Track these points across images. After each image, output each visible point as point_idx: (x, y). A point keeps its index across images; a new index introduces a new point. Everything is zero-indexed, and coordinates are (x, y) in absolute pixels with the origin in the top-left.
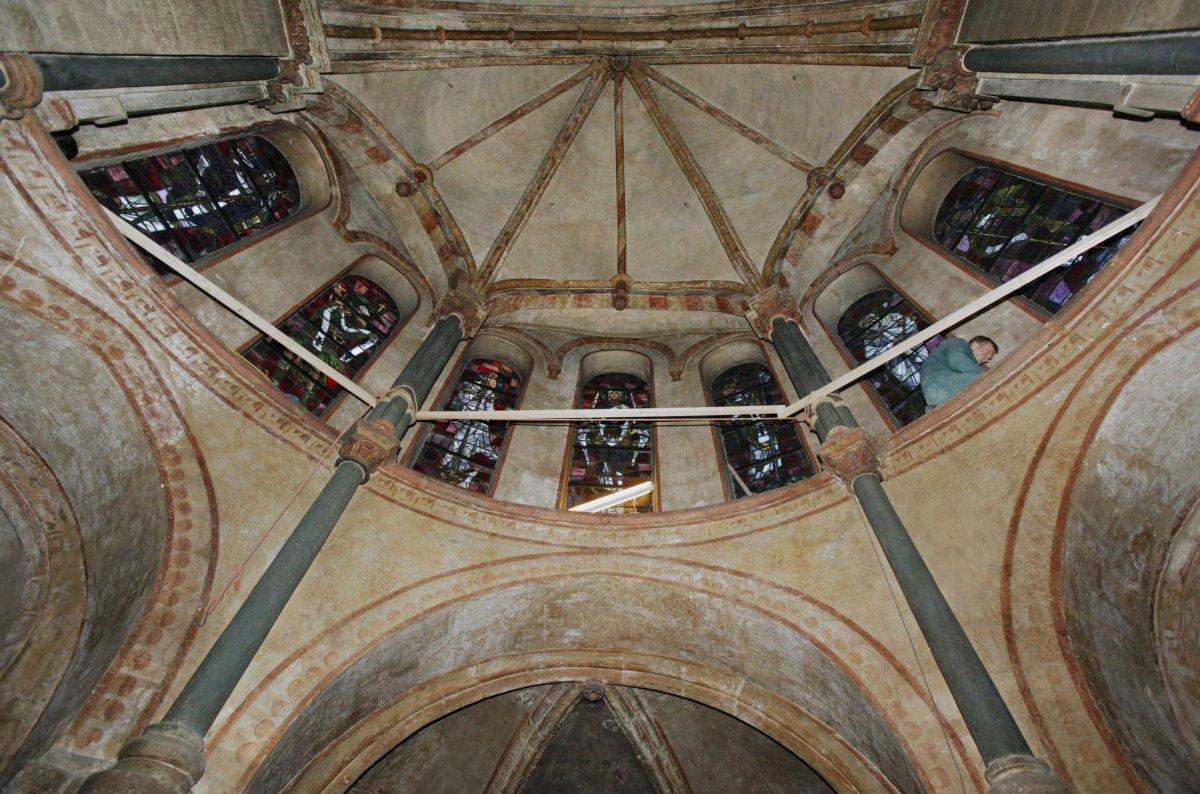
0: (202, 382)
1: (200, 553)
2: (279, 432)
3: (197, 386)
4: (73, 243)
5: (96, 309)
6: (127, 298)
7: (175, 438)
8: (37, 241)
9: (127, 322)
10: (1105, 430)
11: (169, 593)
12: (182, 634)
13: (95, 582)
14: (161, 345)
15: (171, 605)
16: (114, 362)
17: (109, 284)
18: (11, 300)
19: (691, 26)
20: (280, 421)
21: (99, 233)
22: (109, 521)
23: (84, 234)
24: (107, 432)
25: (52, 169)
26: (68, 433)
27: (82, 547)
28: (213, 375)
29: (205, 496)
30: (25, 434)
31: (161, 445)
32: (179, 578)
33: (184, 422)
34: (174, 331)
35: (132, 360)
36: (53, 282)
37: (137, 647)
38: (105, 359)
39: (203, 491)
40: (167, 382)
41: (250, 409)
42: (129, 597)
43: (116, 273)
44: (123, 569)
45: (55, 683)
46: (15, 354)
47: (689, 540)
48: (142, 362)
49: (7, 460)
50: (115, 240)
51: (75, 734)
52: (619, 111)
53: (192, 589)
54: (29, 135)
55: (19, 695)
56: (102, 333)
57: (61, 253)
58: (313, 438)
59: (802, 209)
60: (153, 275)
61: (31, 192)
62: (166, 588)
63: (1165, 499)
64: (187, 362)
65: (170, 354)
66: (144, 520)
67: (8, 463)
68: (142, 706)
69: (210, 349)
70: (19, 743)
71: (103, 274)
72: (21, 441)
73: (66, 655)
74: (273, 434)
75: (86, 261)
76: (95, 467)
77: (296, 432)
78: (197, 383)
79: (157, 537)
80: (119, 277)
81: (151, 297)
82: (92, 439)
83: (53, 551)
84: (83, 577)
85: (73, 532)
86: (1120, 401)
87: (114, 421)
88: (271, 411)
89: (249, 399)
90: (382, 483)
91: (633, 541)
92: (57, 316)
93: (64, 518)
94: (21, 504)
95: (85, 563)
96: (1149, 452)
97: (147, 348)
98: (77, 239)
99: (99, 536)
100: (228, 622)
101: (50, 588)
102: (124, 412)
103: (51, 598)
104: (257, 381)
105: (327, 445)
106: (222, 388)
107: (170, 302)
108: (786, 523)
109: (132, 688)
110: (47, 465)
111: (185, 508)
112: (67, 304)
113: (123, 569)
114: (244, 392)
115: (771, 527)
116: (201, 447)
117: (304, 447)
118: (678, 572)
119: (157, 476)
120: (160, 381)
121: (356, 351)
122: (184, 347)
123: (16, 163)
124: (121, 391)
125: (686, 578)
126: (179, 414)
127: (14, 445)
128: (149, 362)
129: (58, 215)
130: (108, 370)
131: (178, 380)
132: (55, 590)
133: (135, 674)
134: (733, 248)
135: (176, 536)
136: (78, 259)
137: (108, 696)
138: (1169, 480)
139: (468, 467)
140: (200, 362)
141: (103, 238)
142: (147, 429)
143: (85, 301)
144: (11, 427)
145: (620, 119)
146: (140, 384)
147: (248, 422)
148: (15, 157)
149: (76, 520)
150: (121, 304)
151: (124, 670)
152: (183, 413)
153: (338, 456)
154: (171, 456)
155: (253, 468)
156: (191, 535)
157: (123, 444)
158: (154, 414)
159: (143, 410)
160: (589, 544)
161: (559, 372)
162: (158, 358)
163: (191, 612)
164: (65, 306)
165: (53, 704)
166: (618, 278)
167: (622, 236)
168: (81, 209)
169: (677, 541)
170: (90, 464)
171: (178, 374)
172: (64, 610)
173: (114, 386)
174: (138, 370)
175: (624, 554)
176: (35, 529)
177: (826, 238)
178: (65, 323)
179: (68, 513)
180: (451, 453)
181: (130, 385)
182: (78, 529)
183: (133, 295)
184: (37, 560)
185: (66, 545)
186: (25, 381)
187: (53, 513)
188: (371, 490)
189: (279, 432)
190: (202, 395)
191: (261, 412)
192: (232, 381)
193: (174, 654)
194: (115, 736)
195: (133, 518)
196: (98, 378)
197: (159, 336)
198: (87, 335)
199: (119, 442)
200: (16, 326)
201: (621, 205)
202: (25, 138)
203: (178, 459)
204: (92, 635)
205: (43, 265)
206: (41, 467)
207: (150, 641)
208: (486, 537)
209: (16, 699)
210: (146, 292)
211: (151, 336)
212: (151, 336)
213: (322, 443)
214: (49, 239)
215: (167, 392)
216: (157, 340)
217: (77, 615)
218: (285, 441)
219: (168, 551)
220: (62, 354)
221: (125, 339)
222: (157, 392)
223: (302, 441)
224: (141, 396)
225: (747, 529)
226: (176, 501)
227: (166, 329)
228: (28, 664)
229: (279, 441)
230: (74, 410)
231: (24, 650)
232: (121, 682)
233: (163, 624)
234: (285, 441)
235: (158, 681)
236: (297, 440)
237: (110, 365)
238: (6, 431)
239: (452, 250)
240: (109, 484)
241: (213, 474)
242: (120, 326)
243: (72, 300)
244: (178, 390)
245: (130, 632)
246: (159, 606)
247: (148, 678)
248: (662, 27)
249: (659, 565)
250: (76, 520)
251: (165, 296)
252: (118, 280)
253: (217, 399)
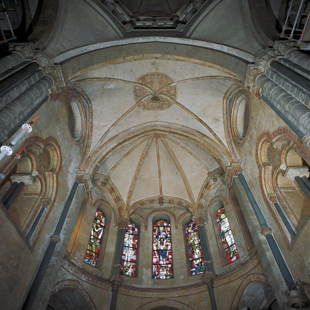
3: (88, 284)
10: (245, 292)
19: (176, 132)
34: (82, 275)
40: (84, 287)
47: (179, 295)
52: (157, 146)
59: (207, 182)
63: (258, 300)
75: (70, 271)
86: (246, 288)
91: (169, 296)
96: (253, 294)
97: (80, 282)
108: (197, 293)
115: (194, 294)
118: (177, 305)
120: (83, 288)
121: (100, 237)
125: (179, 306)
128: (81, 285)
134: (190, 194)
138: (258, 297)
139: (130, 264)
145: (158, 148)
146: (81, 291)
160: (160, 297)
161: (147, 227)
166: (160, 196)
167: (160, 181)
169: (177, 296)
175: (167, 299)
177: (213, 189)
180: (125, 261)
197: (80, 278)
201: (160, 172)
208: (140, 298)
215: (85, 289)
216: (81, 279)
225: (190, 293)
239: (118, 199)
248: (167, 130)
249: (174, 303)
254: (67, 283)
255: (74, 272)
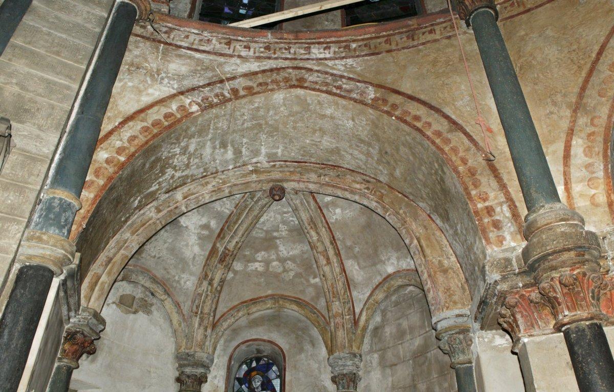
0: (350, 57)
1: (450, 131)
2: (415, 43)
3: (350, 61)
4: (230, 52)
5: (271, 70)
6: (275, 53)
7: (371, 93)
8: (220, 65)
9: (287, 63)
11: (458, 160)
12: (489, 172)
13: (413, 195)
14: (313, 60)
15: (466, 164)
16: (306, 85)
17: (262, 55)
18: (244, 96)
20: (408, 38)
21: (232, 37)
22: (388, 163)
23: (228, 43)
24: (340, 122)
25: (188, 29)
26: (327, 142)
27: (389, 186)
28: (349, 49)
29: (419, 105)
30: (313, 160)
31: (370, 102)
32: (455, 150)
33: (365, 82)
34: (309, 48)
35: (312, 78)
36: (245, 75)
37: (473, 193)
38: (302, 87)
39: (415, 104)
40: (335, 72)
41: (387, 47)
42: (439, 183)
43: (257, 48)
44: (421, 177)
45: (448, 246)
46: (271, 125)
48: (316, 74)
49: (320, 176)
50: (239, 33)
51: (491, 243)
53: (468, 150)
54: (165, 24)
55: (439, 258)
56: (286, 78)
57: (234, 60)
58: (437, 28)
60: (270, 31)
61: (194, 47)
62: (454, 158)
64: (331, 55)
65: (321, 59)
66: (403, 144)
67: (322, 177)
68: (508, 214)
69: (333, 39)
70: (462, 276)
71: (255, 53)
72: (315, 165)
73: (438, 233)
74: (413, 47)
75: (243, 54)
76: (354, 146)
77: (423, 33)
78: (348, 60)
79: (420, 144)
80: (260, 47)
81: (281, 43)
82: (338, 134)
83: (381, 197)
84: (406, 198)
85: (379, 184)
87: (338, 114)
88: (397, 38)
89: (380, 43)
90: (509, 8)
92: (264, 88)
93: (368, 182)
94: (346, 190)
95: (399, 192)
97: (309, 66)
98: (229, 49)
99: (392, 175)
100: (507, 150)
101: (398, 213)
102: (337, 104)
103: (404, 215)
104: (372, 29)
105: (449, 23)
106: (362, 51)
107: (291, 36)
109: (493, 210)
110: (335, 166)
111: (417, 118)
112: (260, 79)
113: (421, 177)
114: (373, 42)
116: (387, 85)
117: (438, 37)
119: (385, 116)
120: (332, 75)
122: (322, 50)
123: (177, 41)
124: (324, 95)
126: (359, 81)
127: (315, 169)
128: (318, 71)
129: (212, 47)
130: (308, 91)
131: (339, 67)
132: (401, 212)
133: (487, 204)
135: (429, 133)
136: (240, 57)
137: (486, 220)
140: (337, 50)
141: (235, 38)
142: (355, 100)
143: (264, 71)
144: (306, 162)
146: (327, 84)
147: (394, 54)
148: (174, 38)
149: (374, 178)
150: (276, 59)
151: (480, 206)
152: (360, 79)
153: (463, 22)
154: (380, 102)
155: (425, 71)
156: (436, 127)
157: (353, 120)
158: (349, 91)
159: (342, 93)
162: (318, 66)
163: (480, 159)
164: (261, 81)
165: (458, 253)
168: (214, 34)
170: (350, 146)
171: (336, 65)
172: (415, 217)
173: (318, 96)
174: (318, 79)
176: (363, 195)
178: (270, 87)
179: (368, 178)
181: (325, 89)
182: (380, 181)
183: (275, 50)
184: (380, 206)
185: (383, 191)
186: (287, 135)
187: (362, 183)
188: (507, 19)
189: (415, 43)
190: (357, 63)
191: (394, 44)
192: (360, 44)
193: (496, 184)
194: (511, 233)
195: (398, 150)
196: (309, 101)
197: (307, 56)
198: (282, 84)
199: (351, 122)
200: (258, 109)
202: (166, 27)
203: (385, 101)
204: (440, 216)
205: (235, 72)
206: (335, 169)
207: (476, 185)
209: (440, 261)
210: (277, 43)
211: (304, 60)
212: (304, 60)
213: (444, 25)
214: (222, 59)
215: (342, 77)
216: (308, 59)
217: (424, 216)
218: (423, 44)
219: (433, 143)
220: (285, 105)
221: (297, 72)
222: (338, 81)
223: (432, 35)
224: (334, 88)
226: (408, 119)
227: (305, 50)
228: (428, 246)
229: (420, 47)
230: (317, 127)
231: (419, 242)
232: (485, 211)
233: (473, 175)
234: (423, 44)
235: (503, 199)
236: (429, 37)
237: (306, 88)
238: (306, 166)
240: (369, 146)
241: (409, 92)
242: (288, 68)
243: (260, 75)
244: (344, 71)
245: (461, 190)
246: (461, 168)
247: (496, 201)
250: (374, 178)
251: (285, 36)
252: (262, 50)
253: (366, 58)
254: (240, 83)
255: (262, 52)
